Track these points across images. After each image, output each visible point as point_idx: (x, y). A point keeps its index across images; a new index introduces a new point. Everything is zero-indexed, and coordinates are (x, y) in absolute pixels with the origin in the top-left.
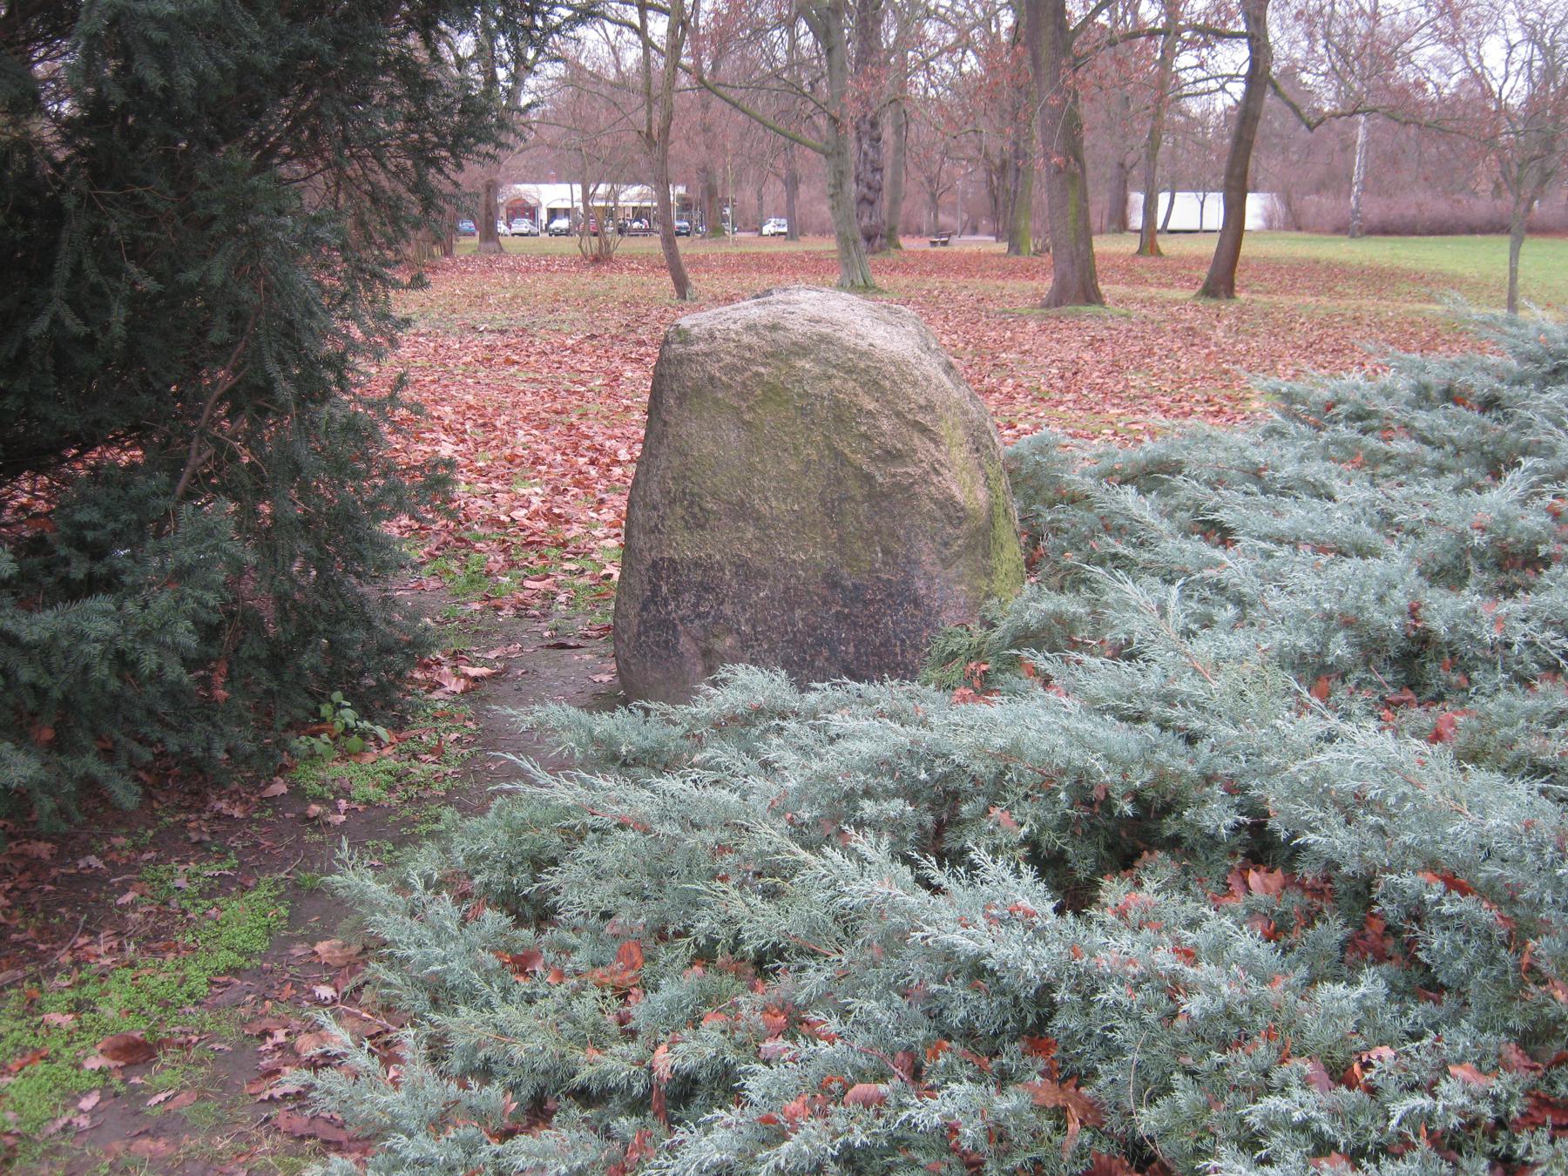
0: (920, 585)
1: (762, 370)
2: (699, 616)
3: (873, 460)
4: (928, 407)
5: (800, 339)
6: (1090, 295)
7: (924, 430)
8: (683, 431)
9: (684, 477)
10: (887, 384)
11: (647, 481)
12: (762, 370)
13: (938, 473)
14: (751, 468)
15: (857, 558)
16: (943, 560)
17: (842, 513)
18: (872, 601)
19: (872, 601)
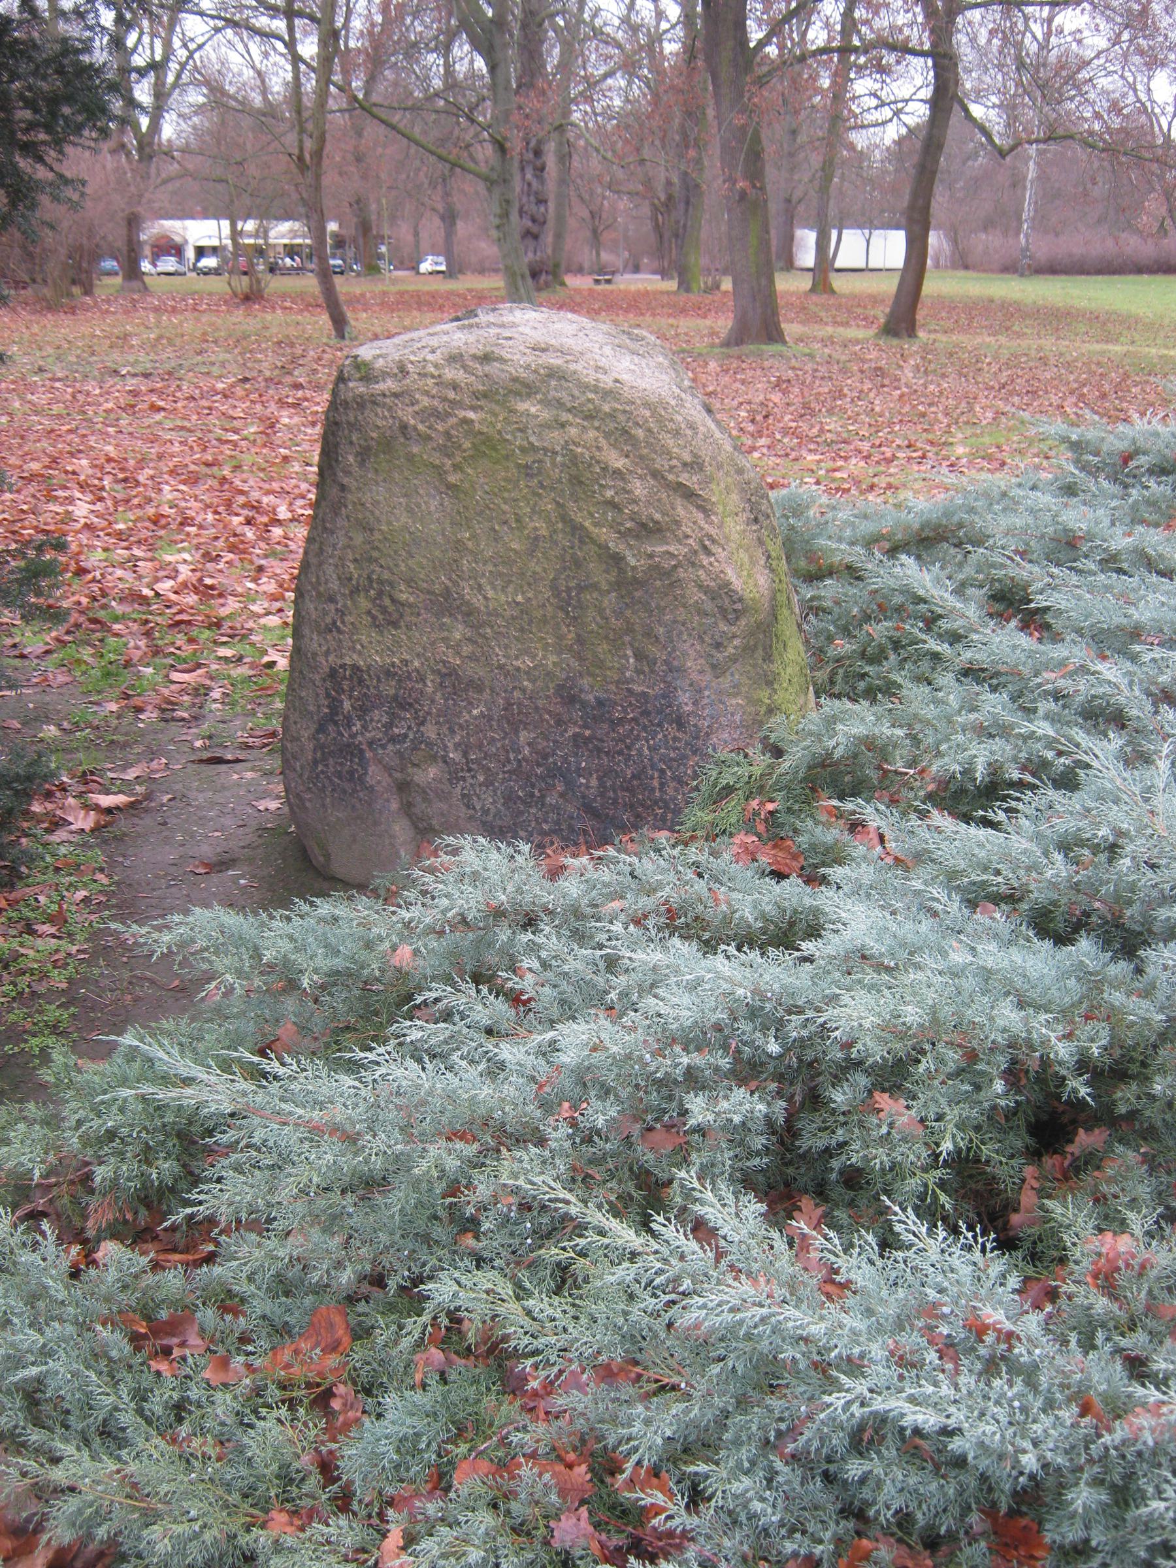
0: (684, 699)
1: (471, 415)
2: (393, 739)
3: (624, 535)
4: (695, 465)
5: (523, 374)
6: (772, 333)
7: (689, 495)
8: (367, 498)
9: (371, 560)
10: (640, 433)
11: (321, 564)
12: (471, 415)
13: (709, 553)
14: (459, 546)
15: (601, 664)
16: (714, 667)
17: (581, 606)
19: (621, 721)
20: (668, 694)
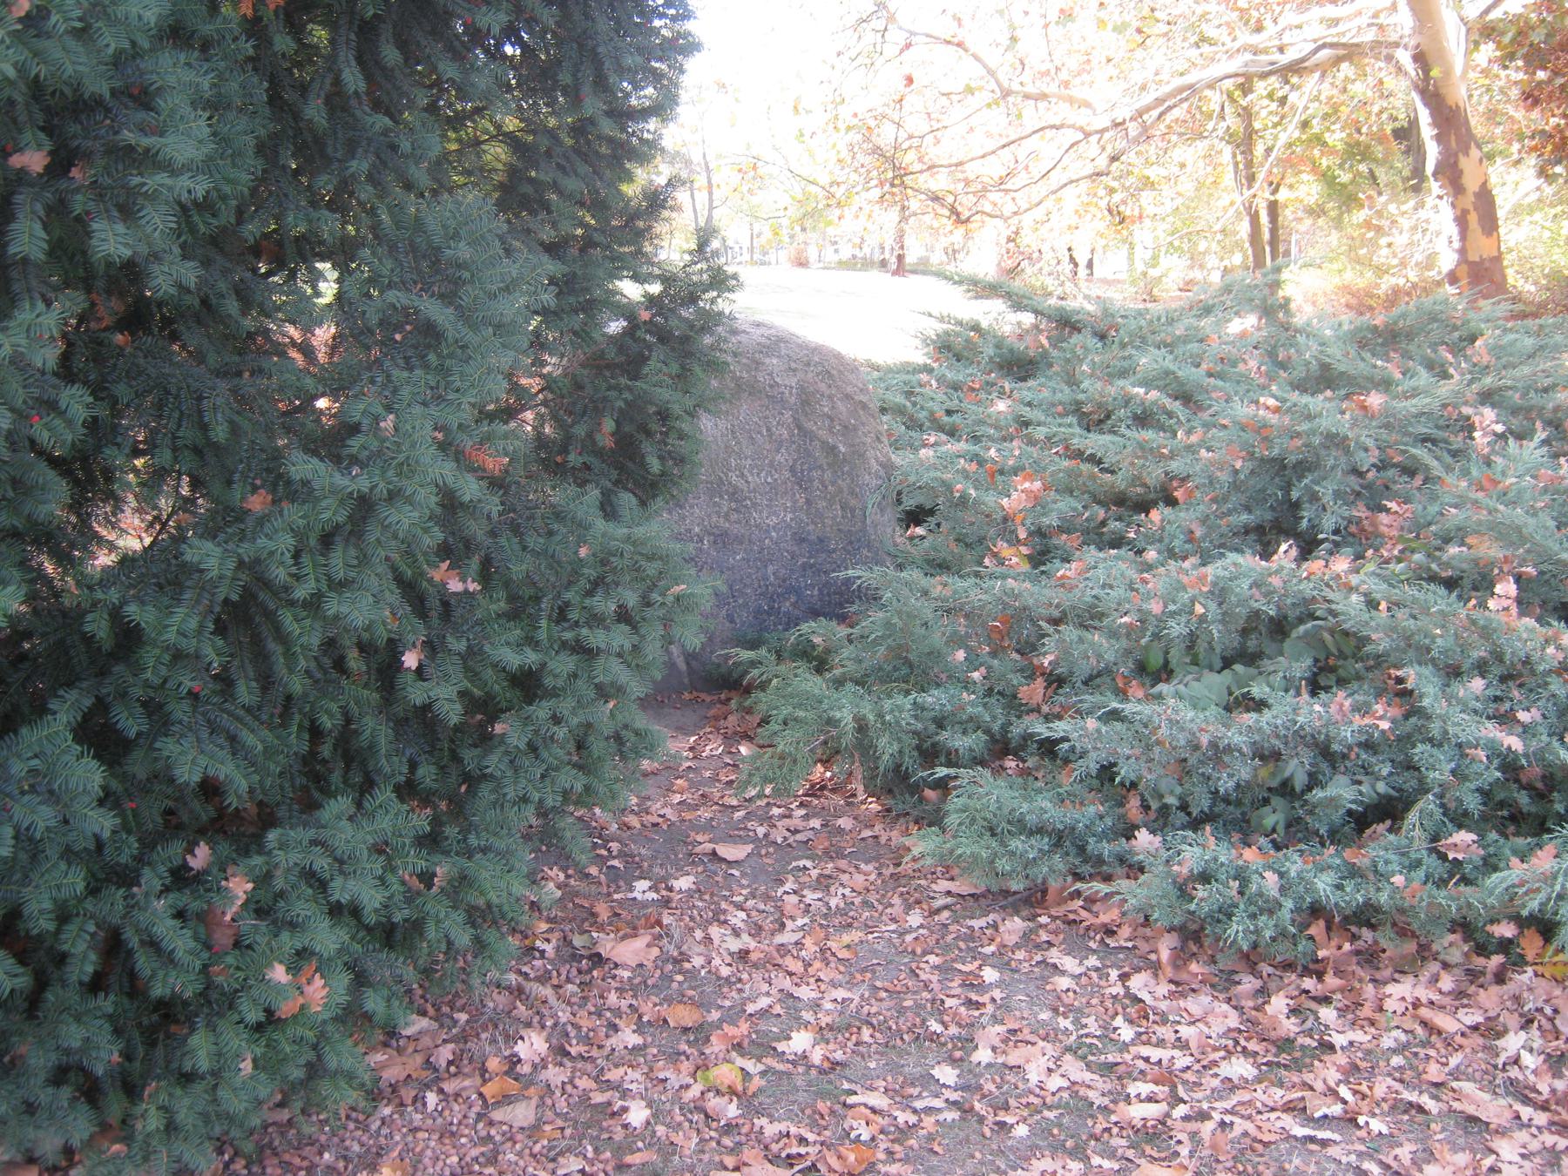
0: (870, 530)
5: (763, 340)
18: (834, 551)
19: (834, 551)
20: (864, 530)
